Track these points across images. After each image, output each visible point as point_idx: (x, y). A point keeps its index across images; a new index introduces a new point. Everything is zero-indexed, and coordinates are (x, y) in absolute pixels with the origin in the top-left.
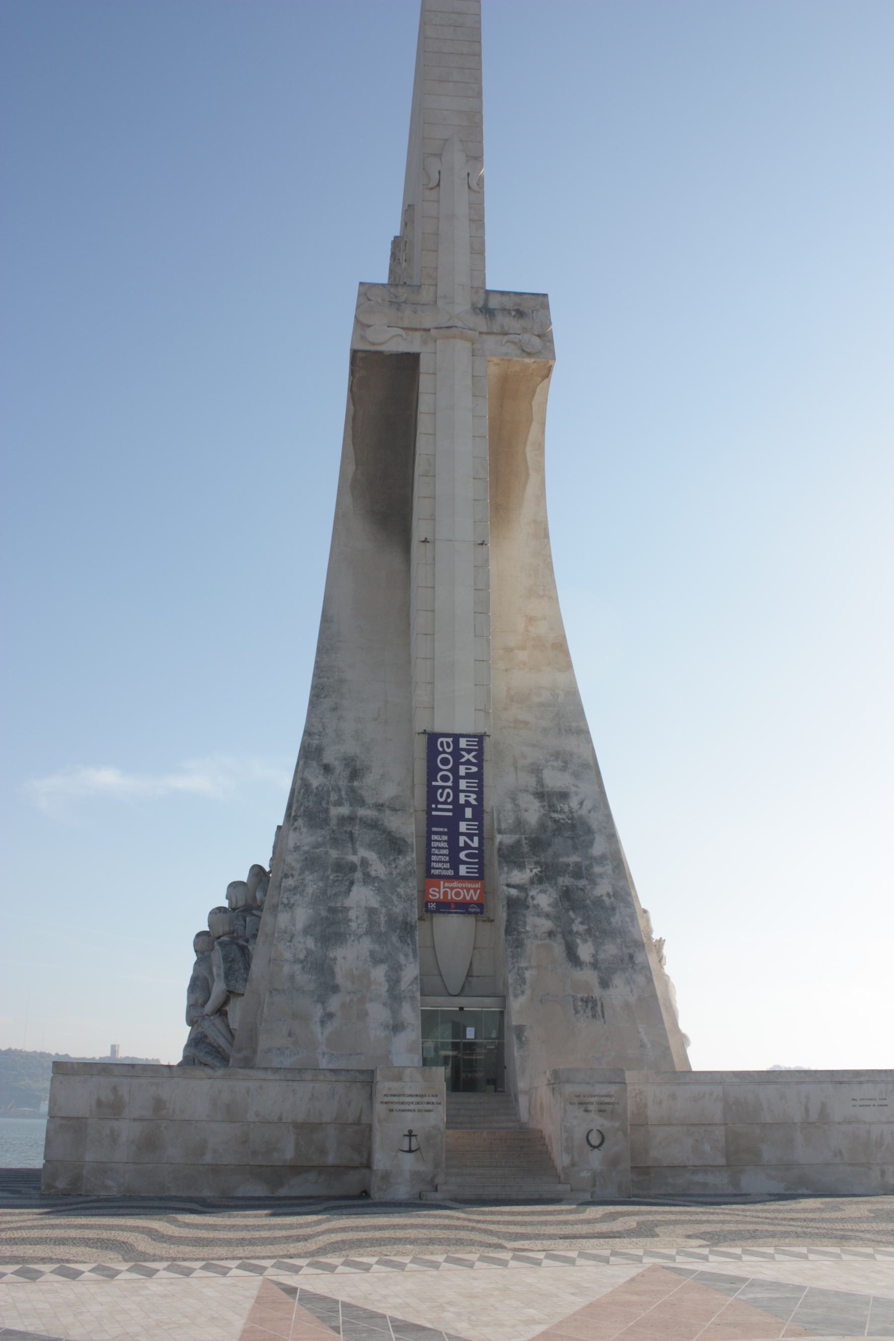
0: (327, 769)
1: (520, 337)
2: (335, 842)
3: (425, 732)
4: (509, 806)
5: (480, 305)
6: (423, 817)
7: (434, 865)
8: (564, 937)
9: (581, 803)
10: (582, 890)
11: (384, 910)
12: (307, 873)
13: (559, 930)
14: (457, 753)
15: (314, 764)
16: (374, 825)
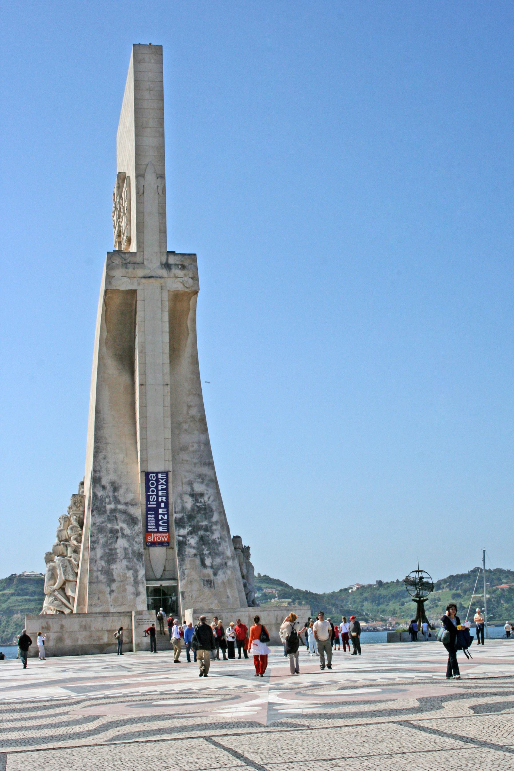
0: (104, 488)
1: (183, 279)
2: (110, 520)
3: (144, 471)
4: (179, 501)
5: (164, 261)
6: (144, 507)
7: (149, 527)
8: (200, 556)
9: (209, 498)
10: (208, 536)
11: (130, 549)
12: (100, 534)
13: (198, 553)
14: (157, 480)
15: (98, 485)
16: (125, 512)
